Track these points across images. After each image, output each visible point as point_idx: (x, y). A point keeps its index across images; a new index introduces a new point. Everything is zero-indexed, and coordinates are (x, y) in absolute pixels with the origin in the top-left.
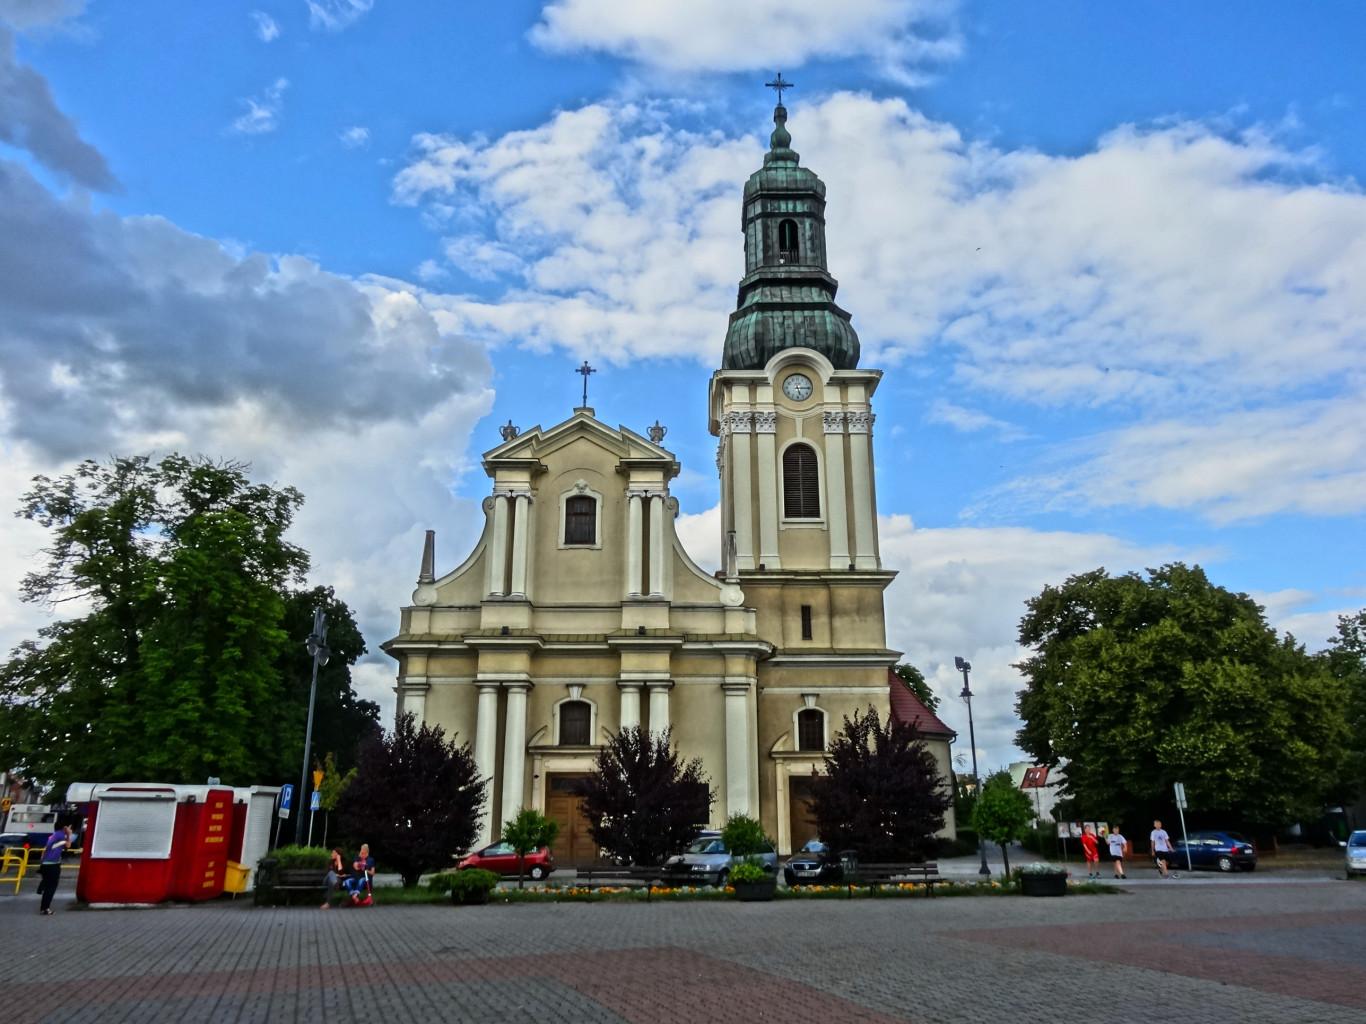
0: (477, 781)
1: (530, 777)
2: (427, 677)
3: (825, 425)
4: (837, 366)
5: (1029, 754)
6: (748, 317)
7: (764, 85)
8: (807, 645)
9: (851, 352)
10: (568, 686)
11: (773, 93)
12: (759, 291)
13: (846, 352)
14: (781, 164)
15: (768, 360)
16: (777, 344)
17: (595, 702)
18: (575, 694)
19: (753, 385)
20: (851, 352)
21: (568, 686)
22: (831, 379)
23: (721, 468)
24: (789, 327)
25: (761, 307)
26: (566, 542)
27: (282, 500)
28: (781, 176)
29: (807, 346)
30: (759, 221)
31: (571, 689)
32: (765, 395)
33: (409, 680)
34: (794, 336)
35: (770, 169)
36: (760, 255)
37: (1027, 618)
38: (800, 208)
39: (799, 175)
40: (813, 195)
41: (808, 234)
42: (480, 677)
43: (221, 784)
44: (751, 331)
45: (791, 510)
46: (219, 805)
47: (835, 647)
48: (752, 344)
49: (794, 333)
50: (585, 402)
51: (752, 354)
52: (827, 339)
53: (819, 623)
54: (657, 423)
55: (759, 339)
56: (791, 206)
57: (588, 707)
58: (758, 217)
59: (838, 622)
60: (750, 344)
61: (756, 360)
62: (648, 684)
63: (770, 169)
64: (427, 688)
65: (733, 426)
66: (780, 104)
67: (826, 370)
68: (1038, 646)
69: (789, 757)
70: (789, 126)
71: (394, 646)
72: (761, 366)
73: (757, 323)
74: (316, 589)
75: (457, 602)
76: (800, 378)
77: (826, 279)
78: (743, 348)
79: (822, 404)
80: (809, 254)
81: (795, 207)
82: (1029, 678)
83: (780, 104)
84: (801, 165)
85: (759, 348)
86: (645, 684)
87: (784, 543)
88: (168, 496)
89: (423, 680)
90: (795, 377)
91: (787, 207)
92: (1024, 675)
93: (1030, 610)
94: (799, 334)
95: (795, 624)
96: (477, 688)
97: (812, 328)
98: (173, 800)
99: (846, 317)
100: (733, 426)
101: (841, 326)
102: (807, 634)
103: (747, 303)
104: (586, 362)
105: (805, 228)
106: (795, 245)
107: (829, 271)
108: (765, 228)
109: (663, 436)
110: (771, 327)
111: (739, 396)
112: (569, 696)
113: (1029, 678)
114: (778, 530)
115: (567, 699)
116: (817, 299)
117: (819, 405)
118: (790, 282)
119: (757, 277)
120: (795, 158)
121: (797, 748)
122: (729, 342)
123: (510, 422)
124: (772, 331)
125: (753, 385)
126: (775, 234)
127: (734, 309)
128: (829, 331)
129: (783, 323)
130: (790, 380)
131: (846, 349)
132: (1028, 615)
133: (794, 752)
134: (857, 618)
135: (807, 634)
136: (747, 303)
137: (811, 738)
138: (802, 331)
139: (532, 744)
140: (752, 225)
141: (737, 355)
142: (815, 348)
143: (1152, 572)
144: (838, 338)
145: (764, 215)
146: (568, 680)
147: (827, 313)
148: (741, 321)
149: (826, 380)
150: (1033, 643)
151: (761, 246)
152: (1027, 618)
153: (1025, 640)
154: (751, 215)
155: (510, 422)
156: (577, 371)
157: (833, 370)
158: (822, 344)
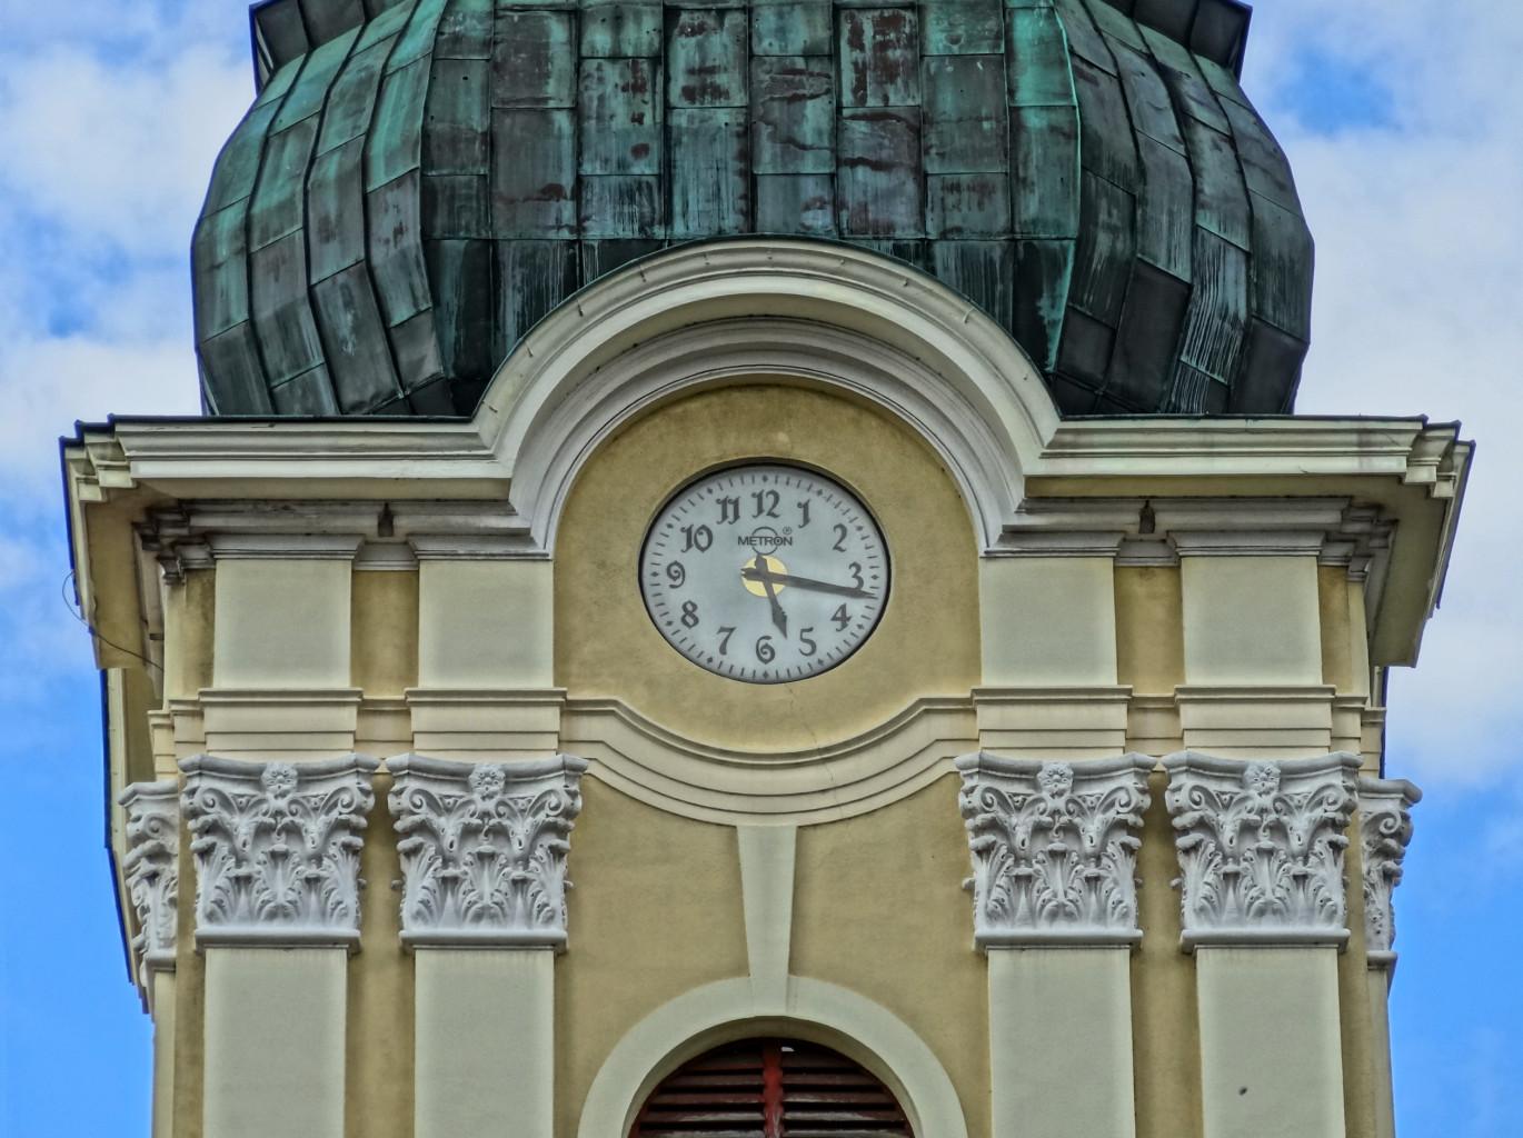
3: (981, 872)
4: (1080, 396)
9: (1231, 291)
13: (1184, 295)
15: (526, 327)
16: (605, 226)
19: (386, 537)
22: (1040, 494)
24: (703, 88)
29: (854, 233)
32: (481, 623)
34: (748, 156)
49: (747, 133)
51: (401, 312)
52: (1016, 183)
60: (384, 226)
61: (428, 360)
65: (209, 882)
67: (999, 406)
72: (461, 394)
76: (791, 491)
78: (333, 261)
79: (966, 707)
85: (454, 247)
90: (743, 488)
94: (792, 144)
97: (900, 98)
100: (209, 882)
101: (1152, 90)
110: (556, 90)
111: (273, 621)
117: (930, 708)
122: (230, 219)
124: (563, 121)
125: (386, 537)
128: (1034, 121)
129: (661, 59)
130: (701, 509)
131: (1182, 271)
138: (815, 115)
141: (285, 320)
142: (918, 255)
144: (1112, 179)
149: (994, 513)
157: (1049, 421)
158: (982, 220)
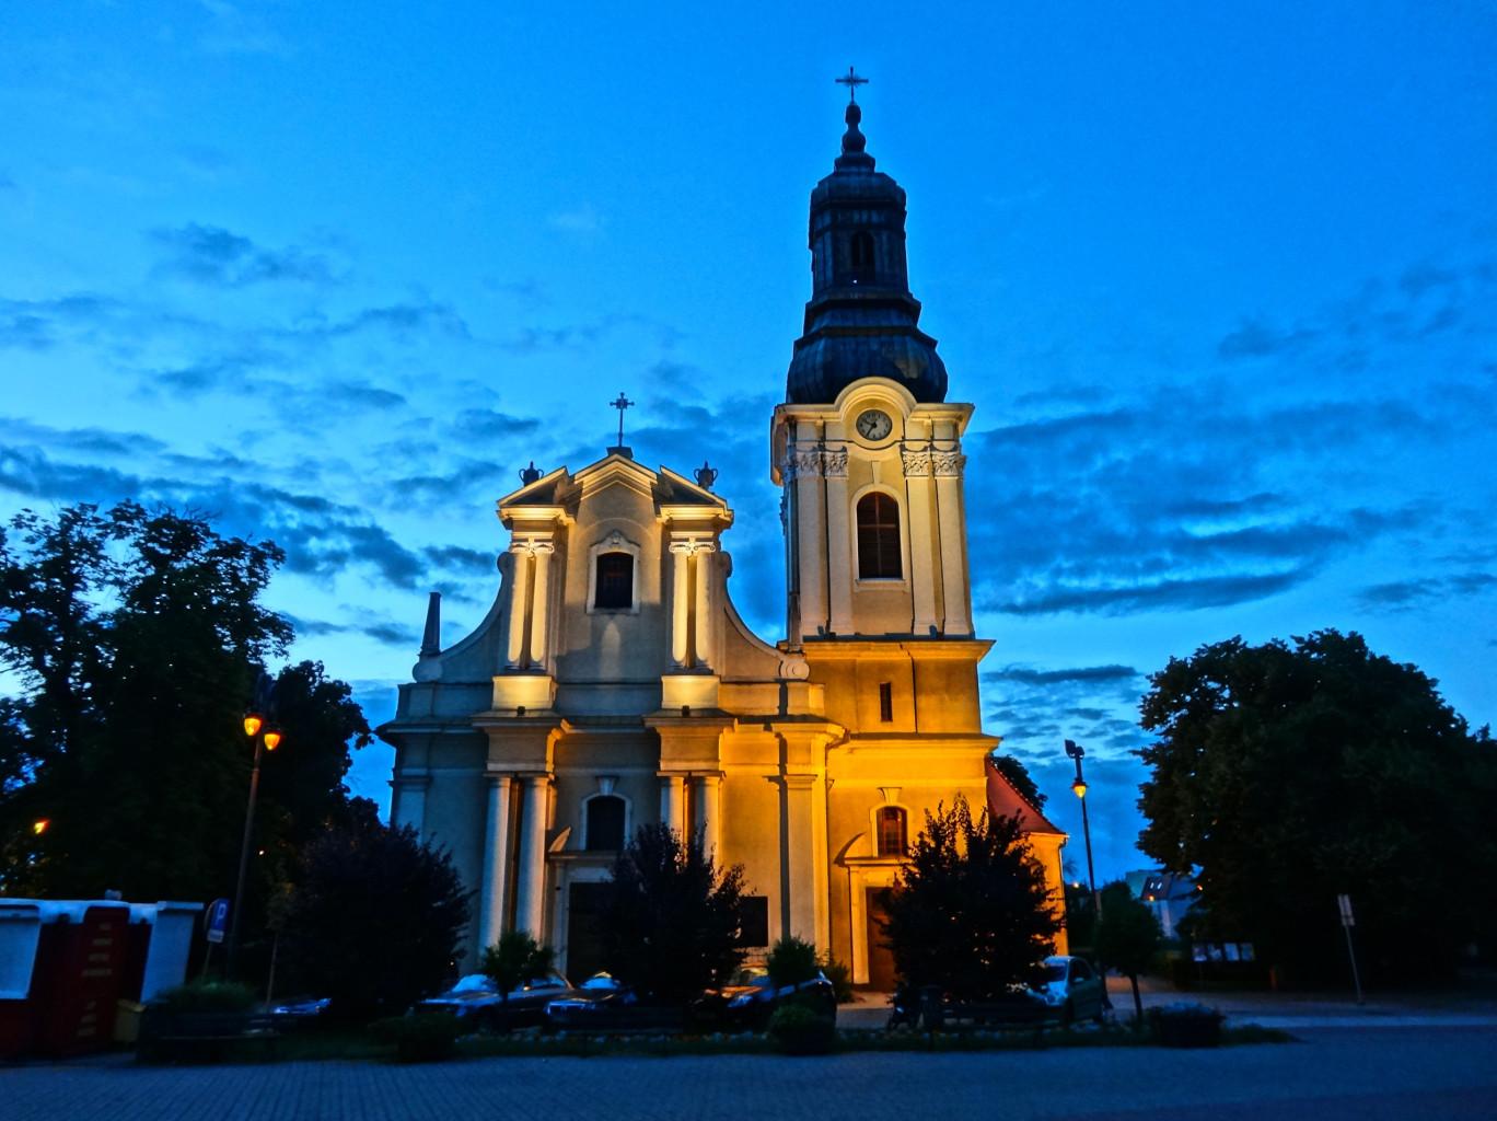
0: (459, 895)
1: (551, 889)
2: (429, 768)
5: (1155, 860)
6: (814, 346)
7: (834, 82)
8: (886, 728)
10: (598, 778)
11: (845, 90)
12: (828, 314)
14: (854, 169)
17: (630, 797)
18: (606, 789)
20: (937, 383)
21: (598, 778)
23: (785, 522)
25: (829, 333)
26: (599, 603)
27: (258, 558)
28: (854, 181)
30: (828, 235)
31: (600, 781)
33: (406, 771)
35: (842, 174)
36: (830, 274)
37: (1149, 697)
38: (875, 218)
39: (874, 180)
40: (889, 203)
41: (885, 247)
42: (491, 767)
43: (122, 900)
44: (819, 359)
45: (868, 569)
46: (105, 927)
47: (920, 731)
48: (820, 374)
50: (620, 440)
53: (902, 701)
54: (706, 464)
55: (828, 367)
56: (865, 217)
57: (621, 803)
58: (825, 229)
59: (923, 701)
62: (694, 774)
63: (842, 174)
64: (427, 783)
66: (853, 102)
68: (1164, 729)
69: (866, 862)
70: (861, 127)
71: (389, 731)
73: (825, 348)
74: (301, 663)
75: (464, 678)
77: (910, 301)
80: (887, 270)
81: (870, 217)
82: (1153, 767)
83: (853, 102)
84: (877, 170)
86: (690, 774)
87: (860, 606)
88: (121, 551)
89: (422, 772)
91: (860, 218)
92: (1148, 763)
93: (1154, 686)
95: (873, 704)
96: (488, 784)
98: (34, 920)
99: (931, 343)
102: (887, 715)
103: (814, 329)
104: (622, 394)
105: (883, 240)
106: (870, 259)
107: (910, 291)
108: (836, 241)
109: (713, 480)
112: (599, 790)
113: (1153, 767)
114: (852, 592)
115: (595, 795)
116: (896, 323)
118: (863, 305)
119: (826, 298)
120: (870, 162)
121: (876, 854)
123: (532, 464)
126: (846, 248)
127: (800, 334)
132: (1150, 694)
133: (871, 858)
134: (946, 697)
135: (887, 715)
136: (814, 329)
137: (891, 844)
139: (551, 850)
140: (820, 239)
143: (1299, 640)
145: (834, 227)
146: (597, 771)
147: (908, 339)
148: (807, 349)
150: (1157, 726)
151: (830, 263)
152: (1149, 697)
153: (1148, 724)
154: (819, 226)
155: (532, 464)
156: (612, 404)
